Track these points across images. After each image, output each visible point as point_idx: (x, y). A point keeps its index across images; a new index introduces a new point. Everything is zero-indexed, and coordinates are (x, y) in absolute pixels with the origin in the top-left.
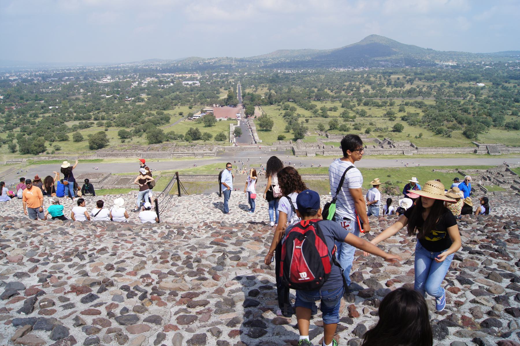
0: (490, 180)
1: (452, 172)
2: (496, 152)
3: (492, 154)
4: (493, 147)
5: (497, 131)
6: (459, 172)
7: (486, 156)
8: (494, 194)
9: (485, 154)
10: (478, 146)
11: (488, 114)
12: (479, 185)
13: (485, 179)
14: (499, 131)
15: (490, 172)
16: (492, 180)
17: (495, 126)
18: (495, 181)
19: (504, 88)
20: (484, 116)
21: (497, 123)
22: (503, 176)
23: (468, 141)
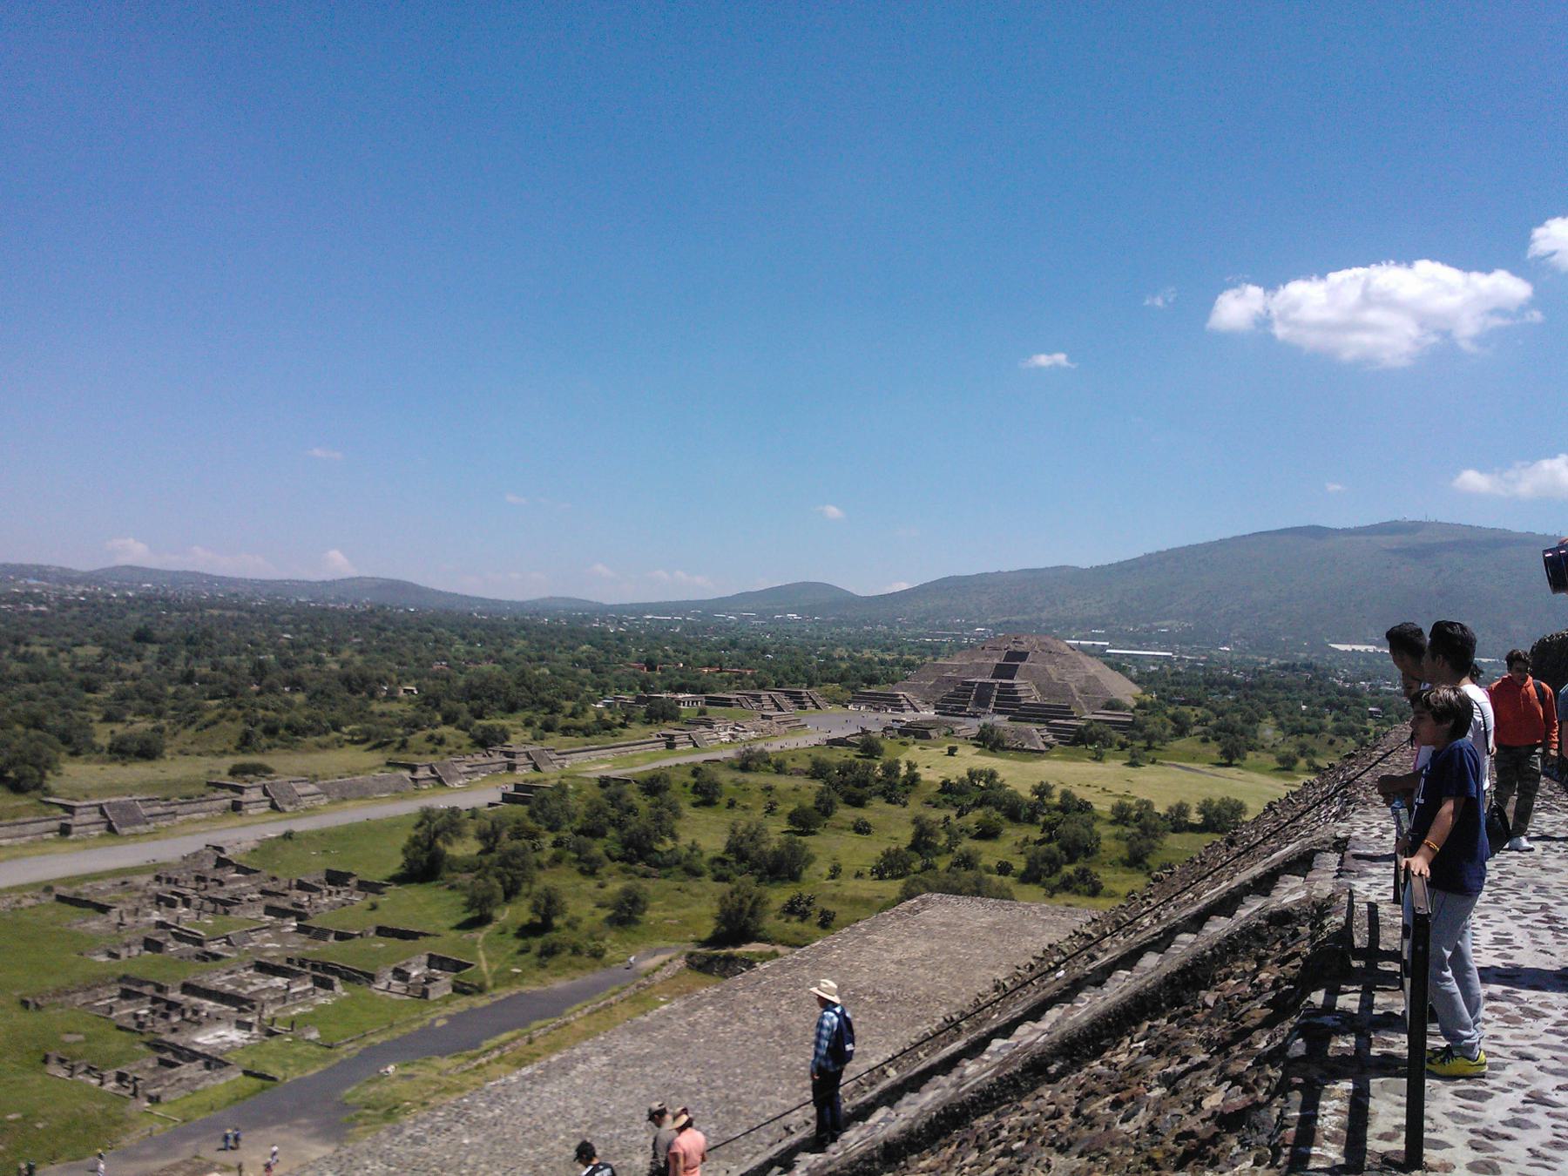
0: (187, 903)
1: (32, 902)
2: (137, 821)
3: (126, 831)
4: (123, 808)
5: (84, 767)
6: (60, 899)
7: (109, 841)
8: (229, 943)
9: (101, 836)
10: (70, 810)
11: (31, 722)
12: (161, 925)
13: (171, 904)
14: (95, 768)
15: (169, 881)
16: (196, 902)
17: (75, 754)
18: (209, 906)
19: (24, 659)
20: (19, 728)
21: (75, 744)
22: (221, 884)
23: (23, 801)
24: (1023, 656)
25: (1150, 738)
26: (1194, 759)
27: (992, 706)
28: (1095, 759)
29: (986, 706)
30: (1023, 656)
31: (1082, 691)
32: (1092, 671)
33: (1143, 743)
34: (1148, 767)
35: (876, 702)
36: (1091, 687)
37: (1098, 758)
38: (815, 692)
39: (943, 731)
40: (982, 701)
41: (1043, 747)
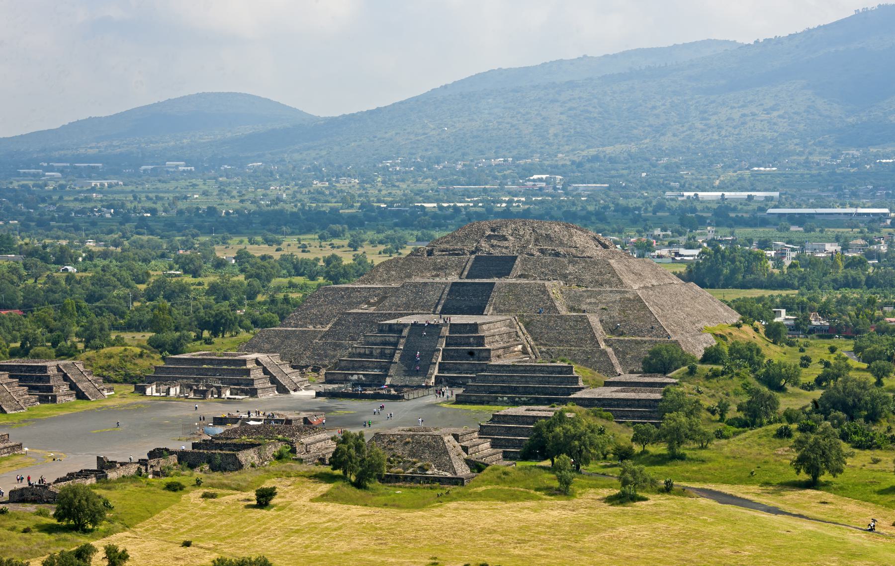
24: (504, 266)
25: (675, 437)
26: (750, 478)
27: (436, 373)
28: (551, 492)
29: (424, 372)
30: (504, 266)
31: (612, 332)
32: (635, 286)
33: (660, 449)
34: (655, 499)
35: (202, 378)
36: (631, 318)
37: (563, 490)
38: (76, 367)
39: (272, 450)
40: (416, 366)
41: (463, 470)
